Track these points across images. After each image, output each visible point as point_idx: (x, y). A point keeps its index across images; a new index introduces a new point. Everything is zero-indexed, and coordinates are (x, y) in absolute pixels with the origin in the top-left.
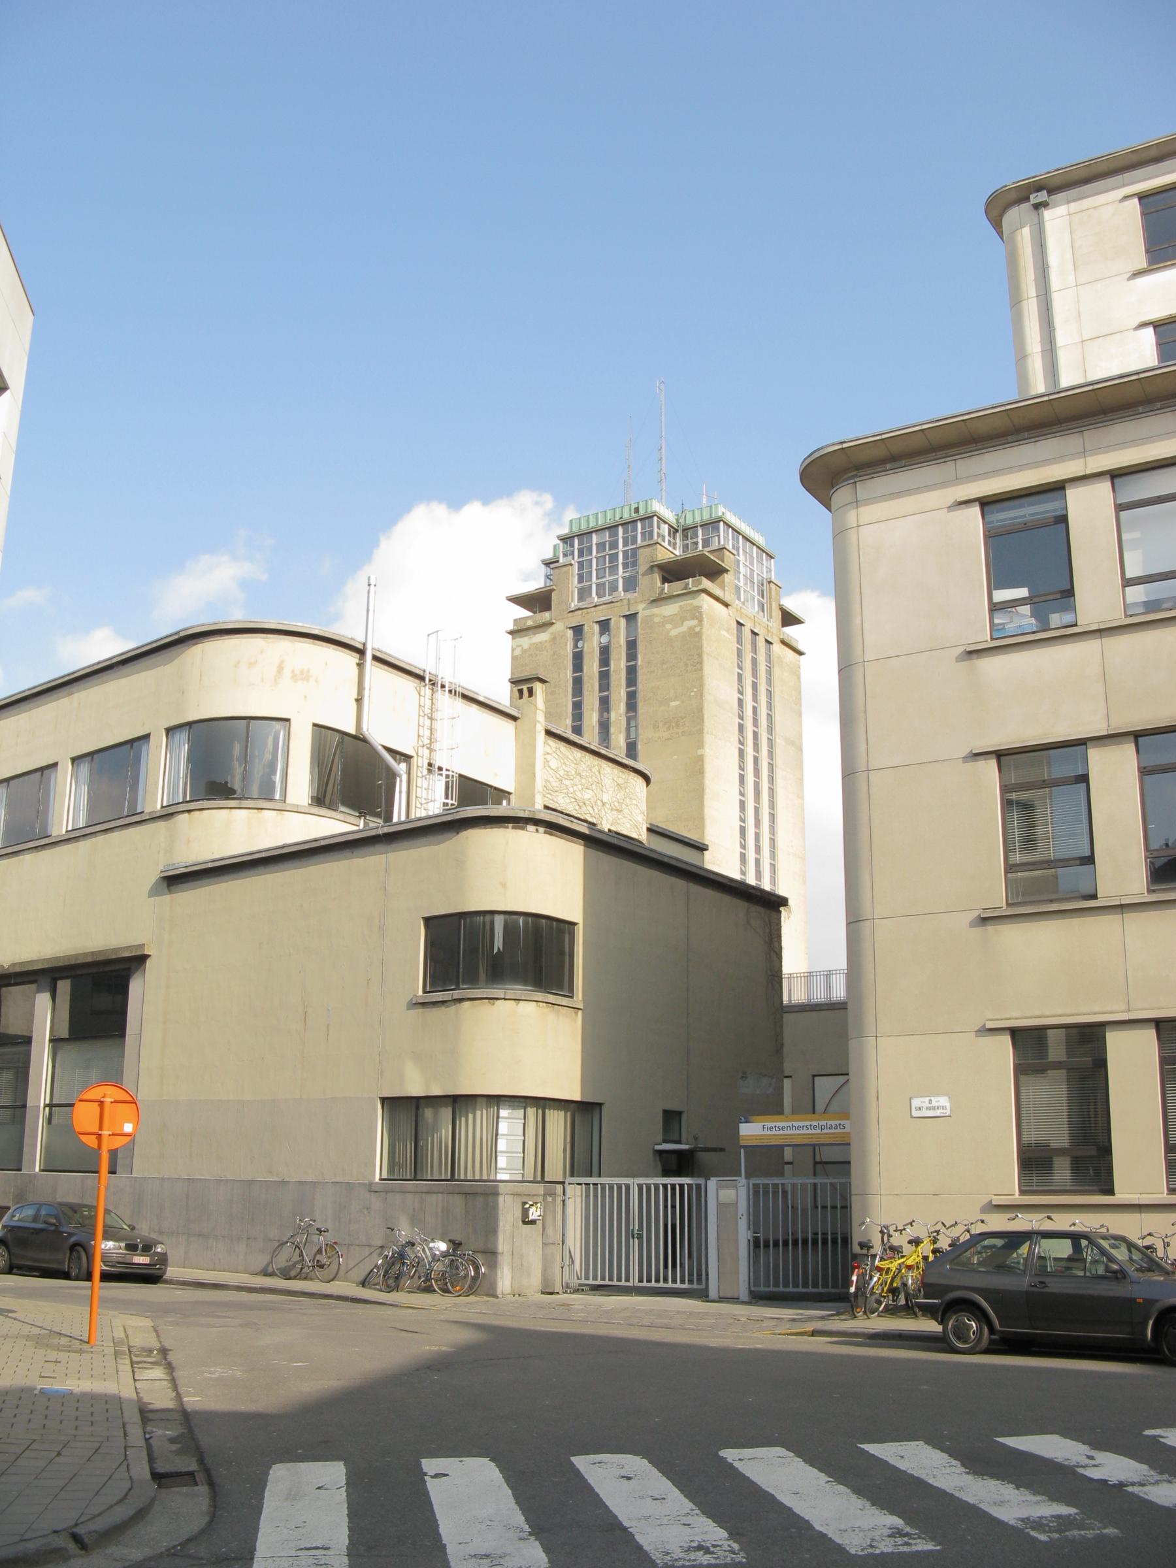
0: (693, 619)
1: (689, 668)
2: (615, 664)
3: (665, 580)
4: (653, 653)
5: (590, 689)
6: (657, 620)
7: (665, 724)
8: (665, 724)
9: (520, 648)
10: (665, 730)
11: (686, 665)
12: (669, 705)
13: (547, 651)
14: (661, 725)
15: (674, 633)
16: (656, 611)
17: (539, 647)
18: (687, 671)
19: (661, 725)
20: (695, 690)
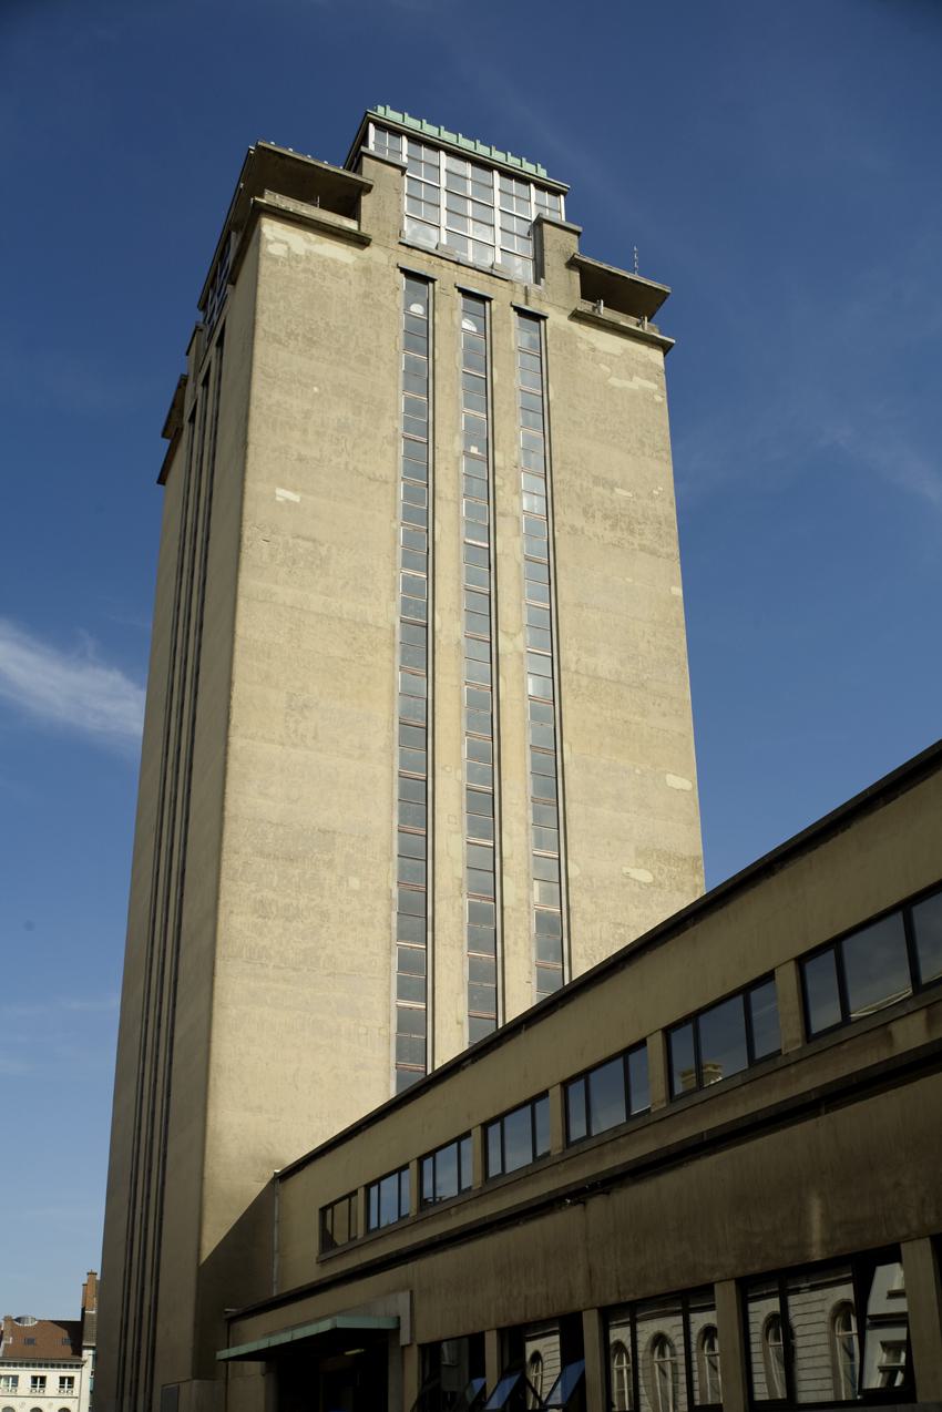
0: (649, 379)
1: (647, 450)
2: (499, 375)
3: (588, 293)
4: (578, 395)
5: (447, 390)
6: (582, 346)
7: (606, 517)
8: (606, 517)
9: (285, 247)
10: (608, 527)
11: (642, 444)
12: (612, 490)
13: (350, 283)
14: (599, 515)
15: (614, 381)
16: (575, 326)
17: (333, 269)
18: (644, 454)
19: (599, 515)
20: (661, 489)
